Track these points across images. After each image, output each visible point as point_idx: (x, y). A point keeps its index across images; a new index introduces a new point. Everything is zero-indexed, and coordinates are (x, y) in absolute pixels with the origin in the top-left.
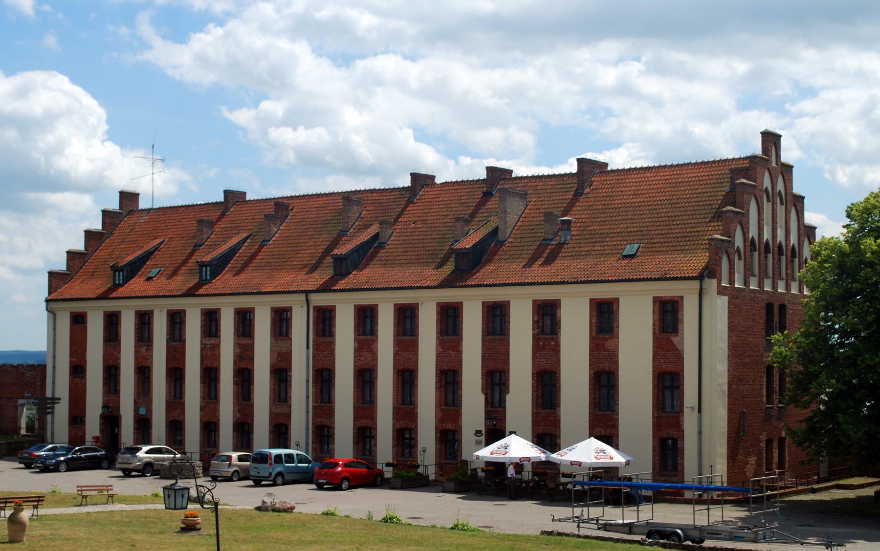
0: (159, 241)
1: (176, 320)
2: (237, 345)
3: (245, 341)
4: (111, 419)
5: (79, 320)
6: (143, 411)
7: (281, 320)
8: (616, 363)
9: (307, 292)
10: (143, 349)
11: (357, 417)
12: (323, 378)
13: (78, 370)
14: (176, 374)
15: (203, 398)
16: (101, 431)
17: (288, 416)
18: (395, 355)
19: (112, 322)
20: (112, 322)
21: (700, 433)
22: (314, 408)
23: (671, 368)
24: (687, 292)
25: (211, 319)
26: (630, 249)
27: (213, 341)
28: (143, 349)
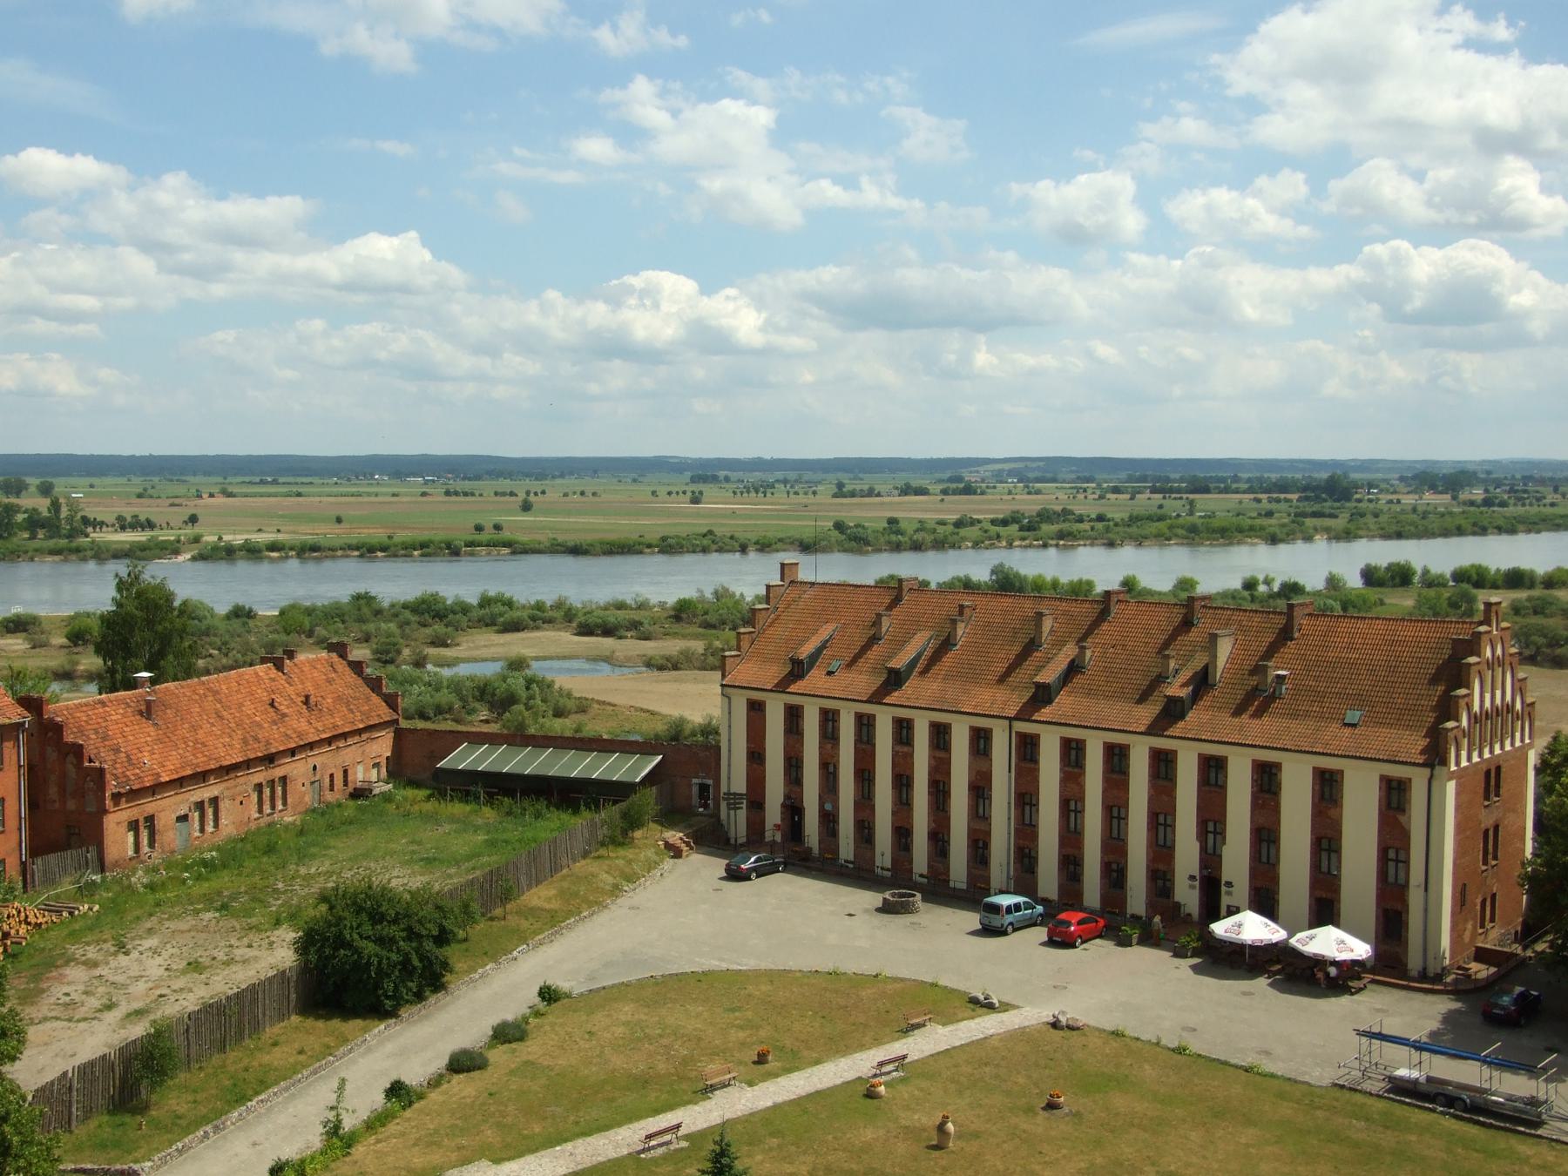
1: (865, 725)
2: (932, 757)
3: (942, 755)
4: (793, 809)
6: (828, 807)
7: (981, 741)
9: (1010, 719)
12: (1026, 799)
13: (756, 756)
14: (865, 775)
15: (894, 804)
16: (783, 819)
20: (793, 716)
22: (1016, 830)
24: (1418, 778)
25: (903, 730)
26: (1353, 716)
27: (906, 749)
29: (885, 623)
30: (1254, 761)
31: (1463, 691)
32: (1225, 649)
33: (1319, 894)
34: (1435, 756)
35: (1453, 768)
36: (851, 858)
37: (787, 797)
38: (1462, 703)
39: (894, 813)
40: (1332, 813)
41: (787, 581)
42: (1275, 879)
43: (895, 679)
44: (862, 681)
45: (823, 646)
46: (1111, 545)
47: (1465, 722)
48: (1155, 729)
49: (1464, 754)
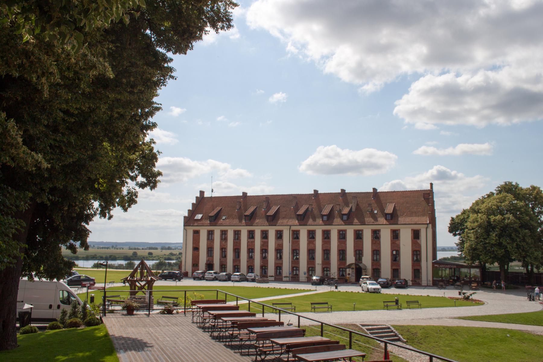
2: (261, 241)
8: (400, 248)
10: (224, 242)
11: (308, 264)
17: (282, 264)
18: (323, 245)
21: (427, 267)
22: (292, 261)
23: (417, 249)
27: (252, 240)
28: (224, 242)
39: (247, 261)
40: (397, 242)
42: (380, 265)
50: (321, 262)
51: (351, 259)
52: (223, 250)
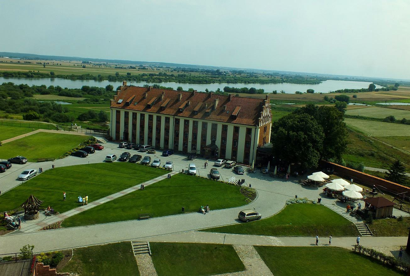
0: (134, 95)
1: (142, 116)
3: (159, 122)
4: (126, 134)
5: (118, 113)
19: (127, 114)
20: (127, 114)
25: (151, 117)
27: (151, 121)
29: (147, 95)
30: (212, 123)
31: (262, 112)
32: (217, 102)
33: (233, 150)
34: (256, 123)
35: (260, 126)
36: (182, 150)
37: (125, 131)
38: (262, 114)
41: (124, 86)
43: (149, 107)
44: (142, 107)
45: (133, 99)
46: (321, 93)
47: (262, 118)
48: (202, 118)
49: (261, 124)
50: (191, 141)
51: (209, 142)
52: (134, 125)
